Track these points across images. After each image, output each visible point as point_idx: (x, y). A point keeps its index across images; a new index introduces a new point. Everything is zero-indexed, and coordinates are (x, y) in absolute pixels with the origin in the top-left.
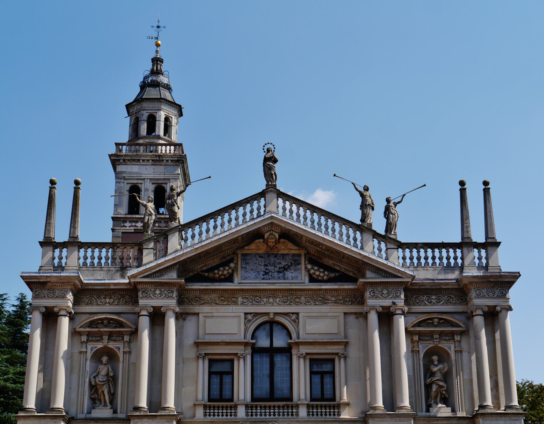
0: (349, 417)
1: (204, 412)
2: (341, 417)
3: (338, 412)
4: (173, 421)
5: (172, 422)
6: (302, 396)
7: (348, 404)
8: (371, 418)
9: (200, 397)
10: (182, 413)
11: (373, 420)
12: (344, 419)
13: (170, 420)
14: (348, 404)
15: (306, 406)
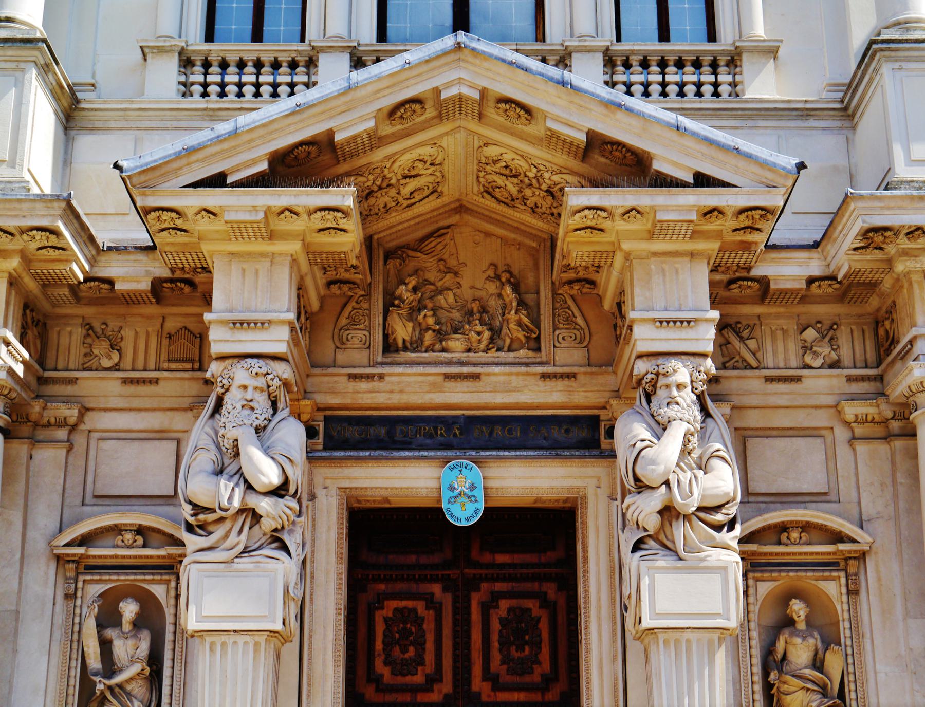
0: (777, 97)
1: (180, 83)
2: (745, 97)
3: (734, 84)
4: (23, 70)
5: (18, 74)
6: (585, 25)
7: (771, 52)
8: (889, 59)
9: (168, 26)
10: (93, 85)
11: (901, 68)
12: (761, 101)
13: (14, 65)
14: (771, 52)
15: (599, 58)
